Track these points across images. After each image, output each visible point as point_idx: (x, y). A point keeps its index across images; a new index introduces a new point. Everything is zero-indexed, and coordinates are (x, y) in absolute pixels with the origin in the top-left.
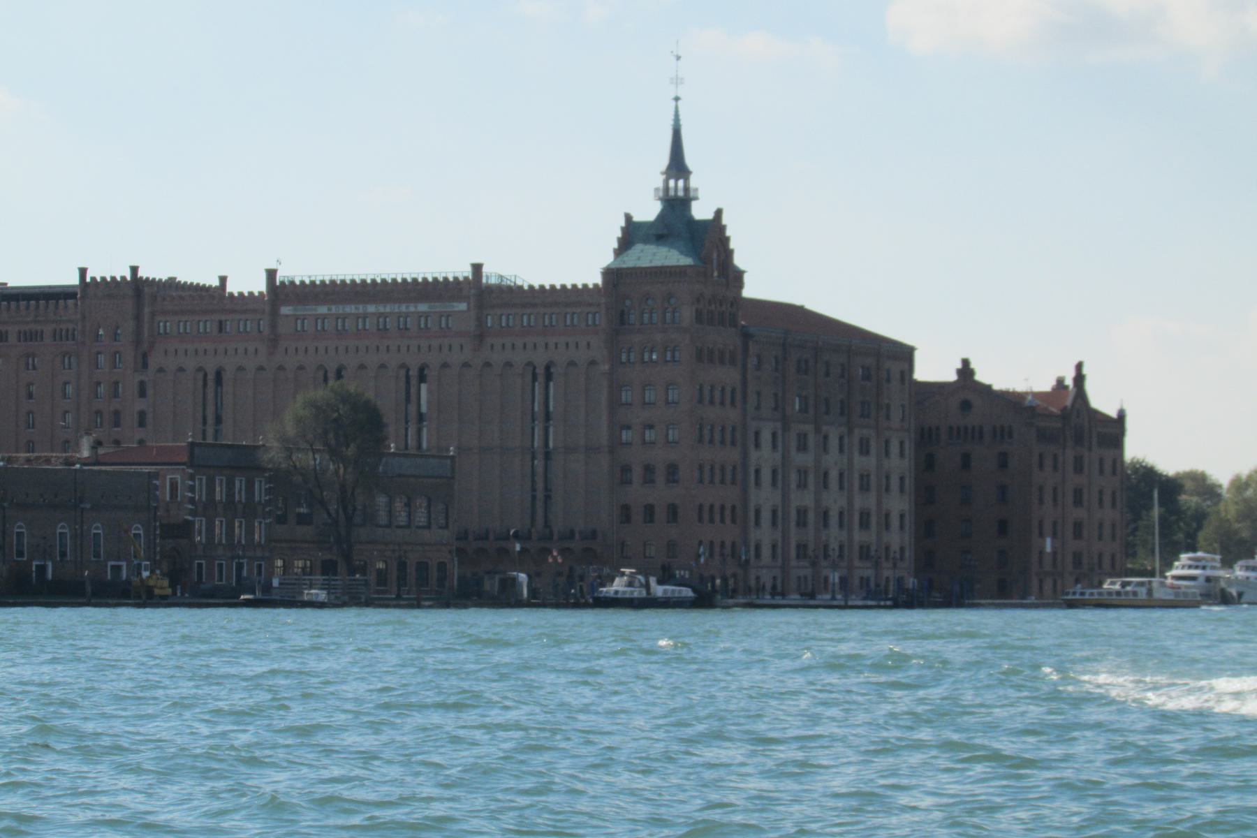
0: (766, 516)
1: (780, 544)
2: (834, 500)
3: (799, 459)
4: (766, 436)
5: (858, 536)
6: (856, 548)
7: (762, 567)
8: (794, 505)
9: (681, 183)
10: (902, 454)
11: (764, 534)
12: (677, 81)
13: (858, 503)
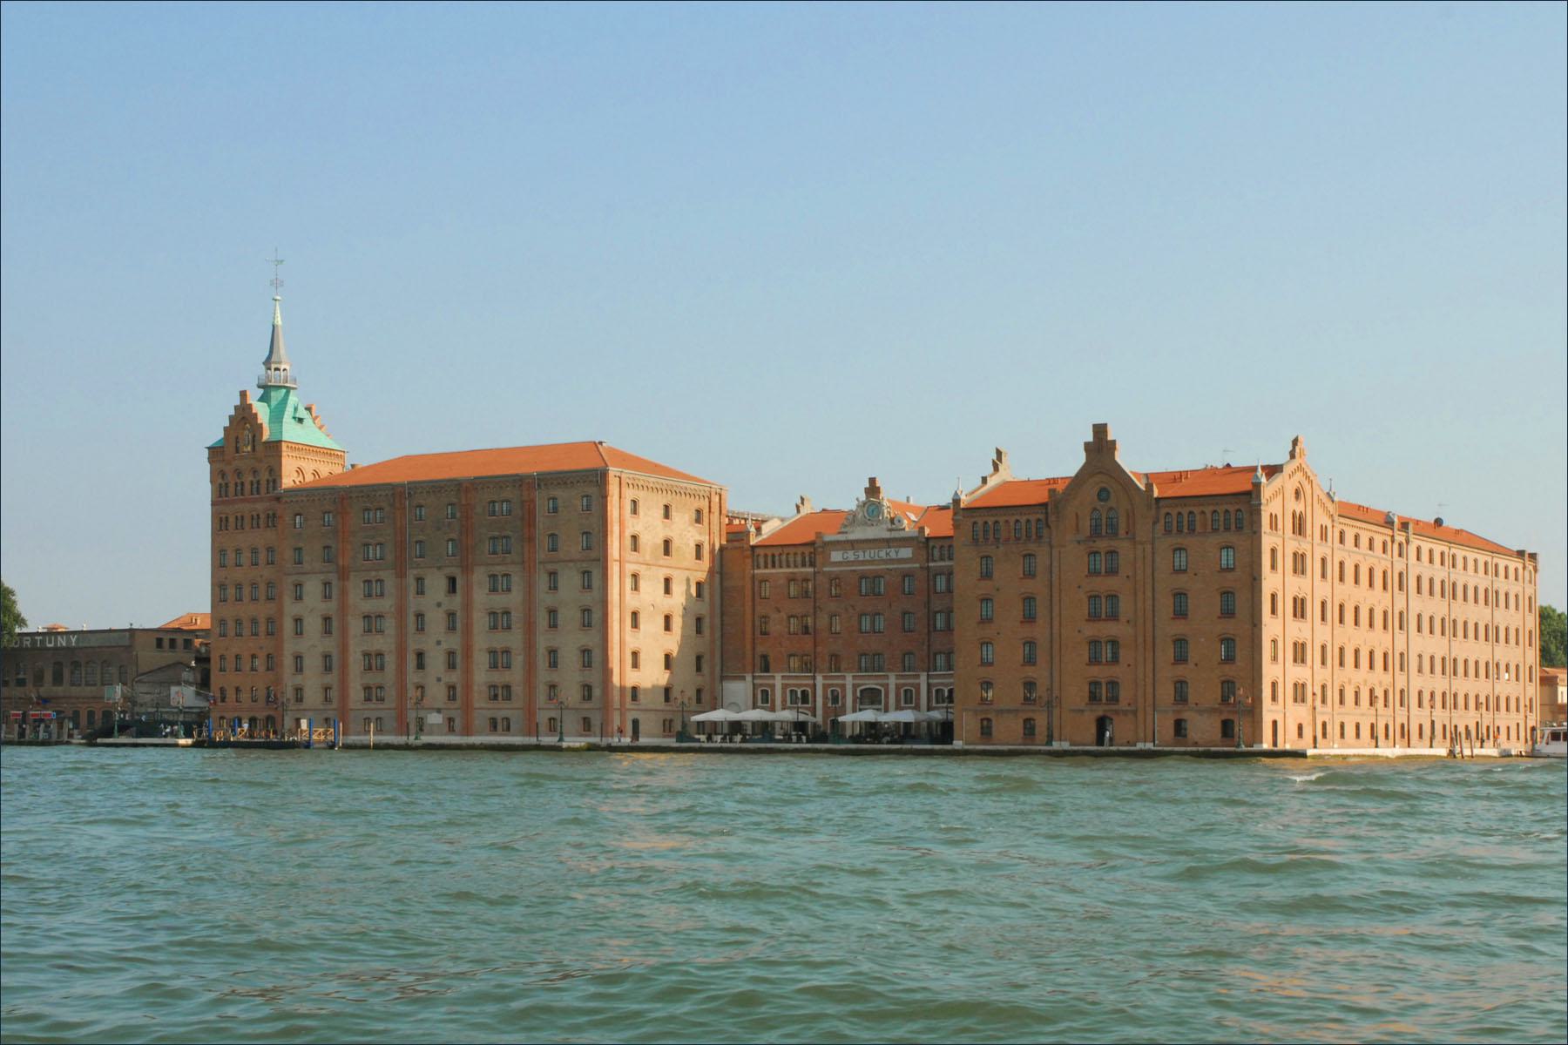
0: (313, 663)
1: (335, 687)
3: (370, 606)
4: (313, 588)
7: (304, 710)
13: (482, 640)
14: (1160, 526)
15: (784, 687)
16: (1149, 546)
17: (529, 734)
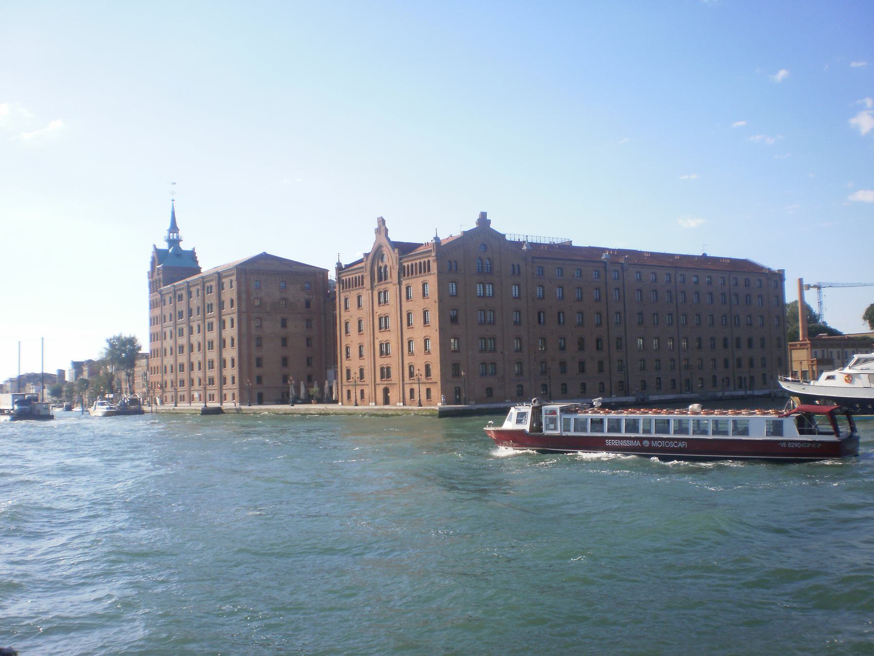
9: (175, 234)
12: (173, 193)
16: (398, 286)
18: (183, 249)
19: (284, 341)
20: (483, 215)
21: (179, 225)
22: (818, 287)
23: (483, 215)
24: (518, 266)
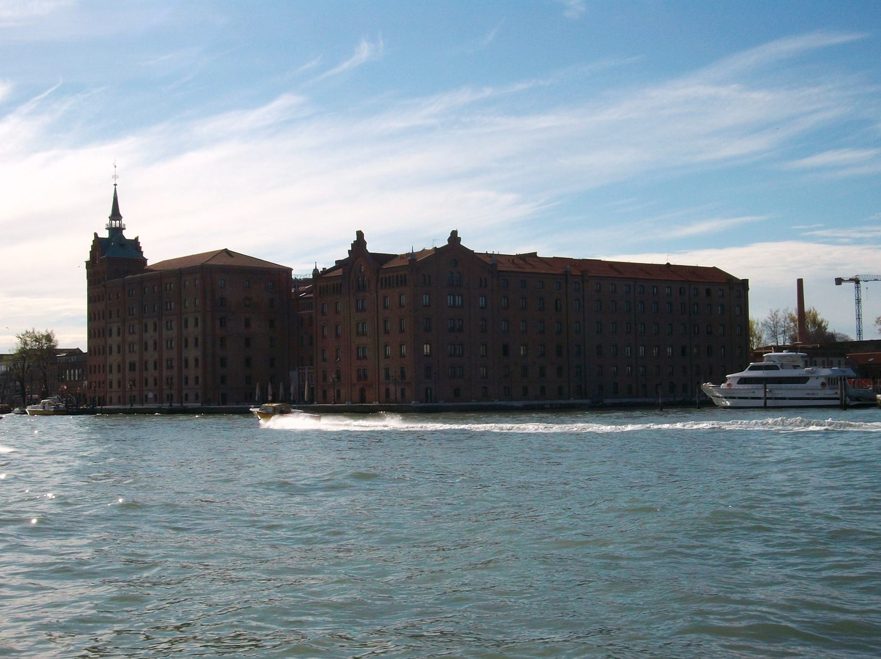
2: (151, 356)
3: (130, 338)
4: (115, 330)
5: (165, 373)
6: (164, 379)
8: (165, 357)
9: (118, 222)
10: (196, 325)
11: (114, 377)
12: (115, 177)
14: (379, 284)
15: (309, 373)
17: (178, 403)
18: (127, 238)
19: (248, 342)
20: (454, 233)
21: (122, 211)
22: (857, 281)
23: (454, 233)
24: (485, 279)
